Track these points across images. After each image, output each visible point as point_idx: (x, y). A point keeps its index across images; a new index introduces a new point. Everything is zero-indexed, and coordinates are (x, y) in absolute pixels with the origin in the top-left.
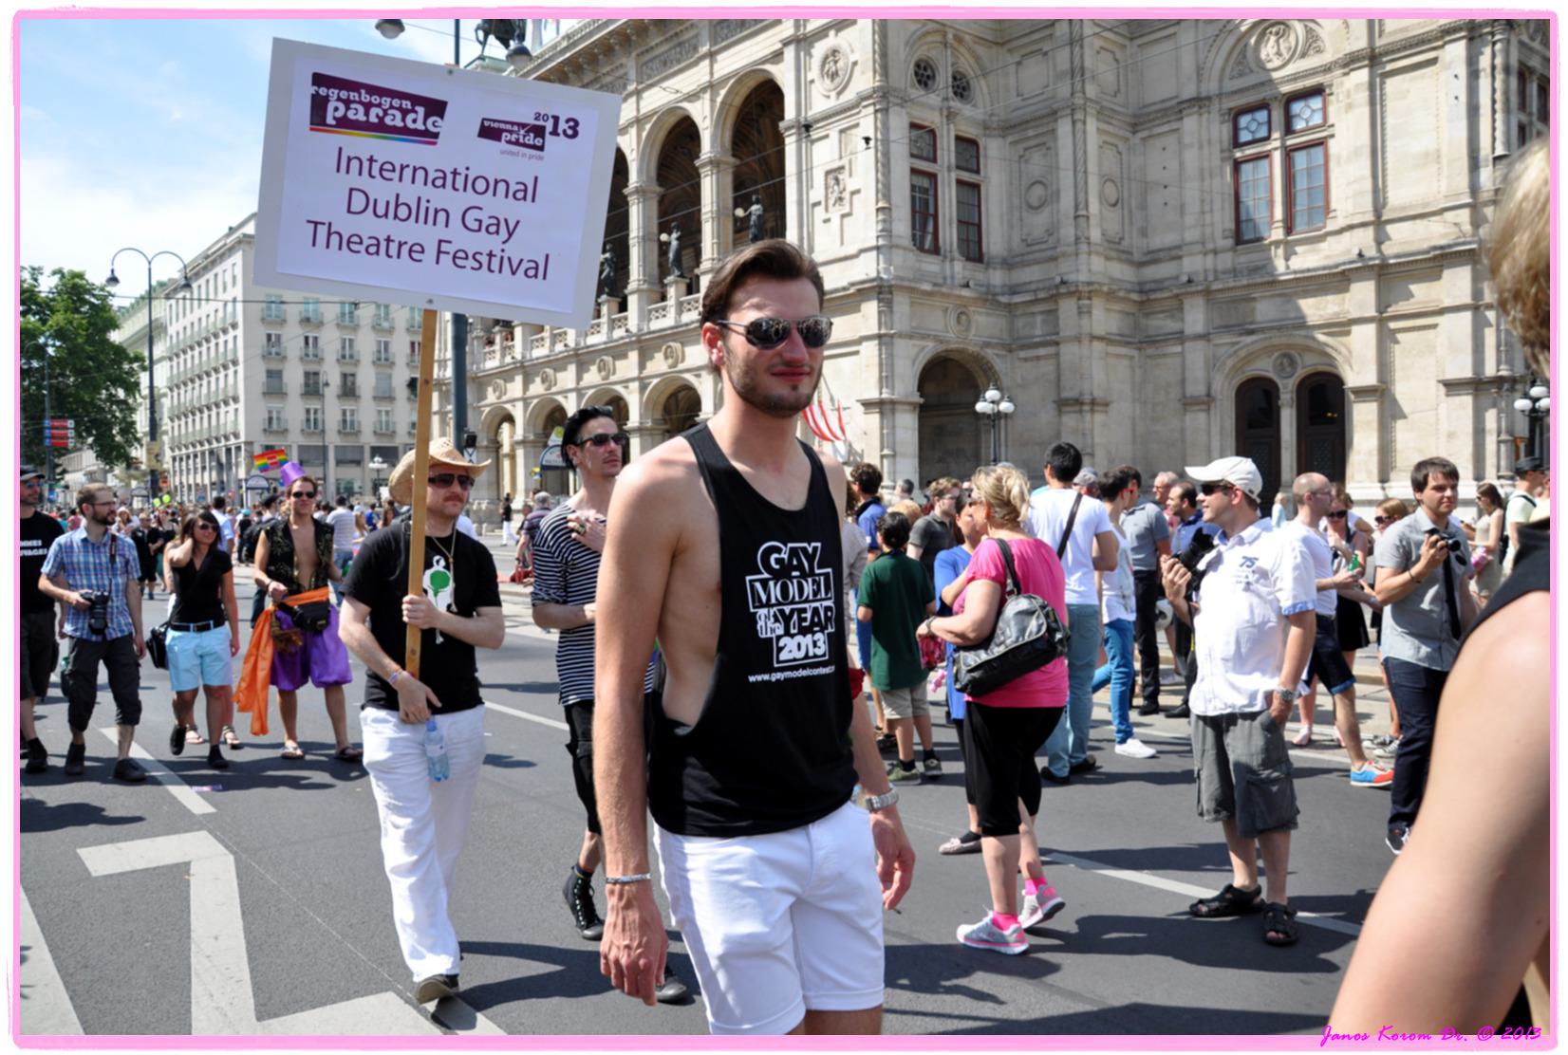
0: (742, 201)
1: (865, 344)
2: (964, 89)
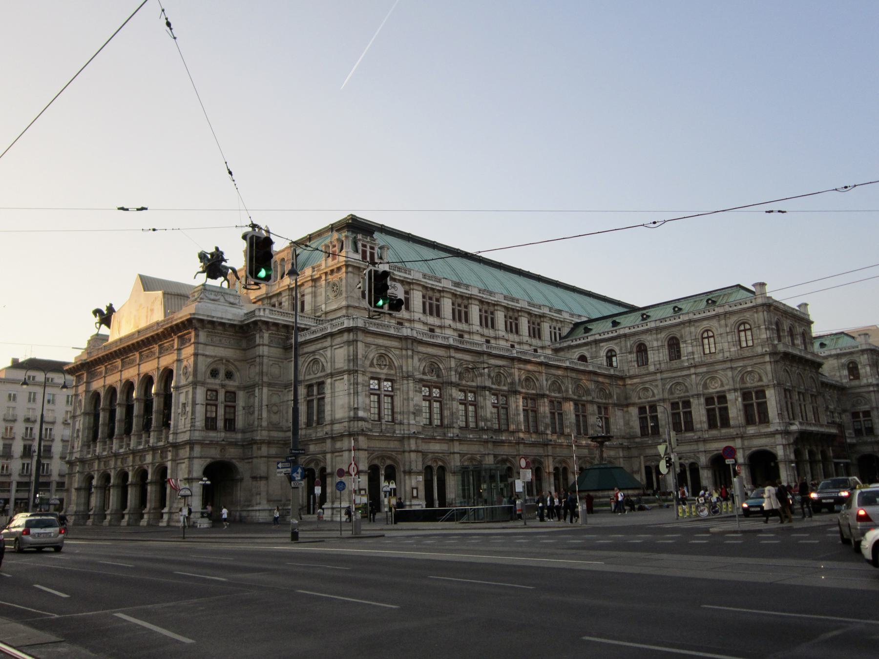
0: (164, 409)
1: (186, 460)
2: (231, 376)
